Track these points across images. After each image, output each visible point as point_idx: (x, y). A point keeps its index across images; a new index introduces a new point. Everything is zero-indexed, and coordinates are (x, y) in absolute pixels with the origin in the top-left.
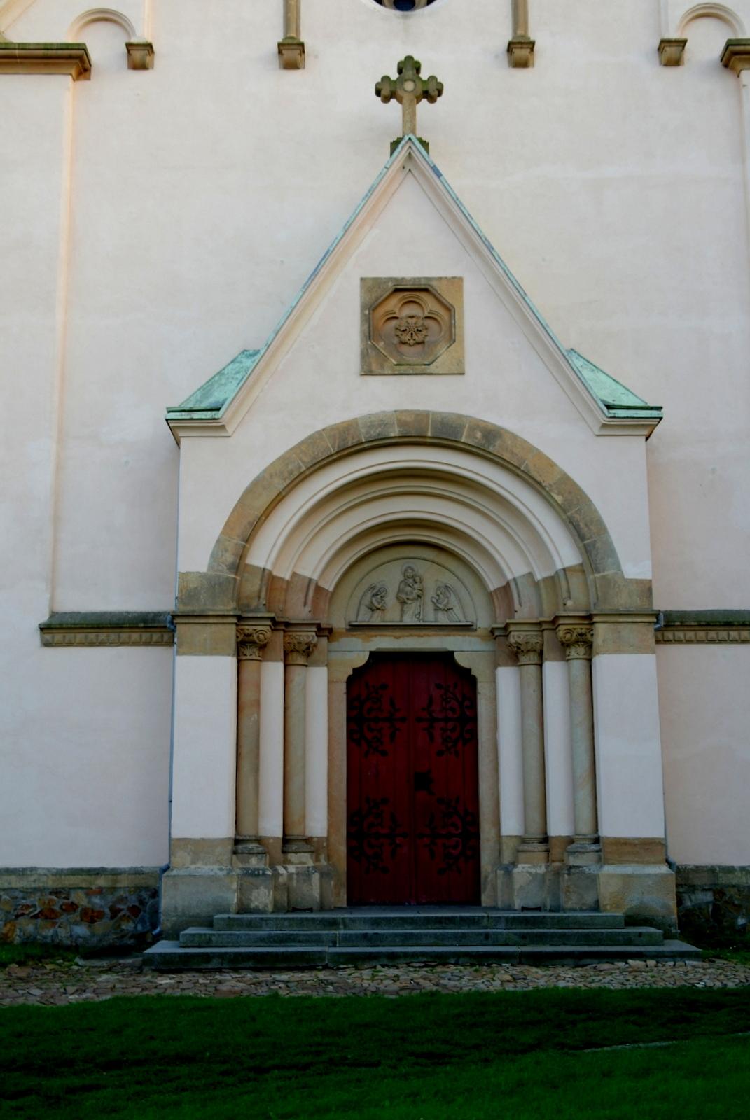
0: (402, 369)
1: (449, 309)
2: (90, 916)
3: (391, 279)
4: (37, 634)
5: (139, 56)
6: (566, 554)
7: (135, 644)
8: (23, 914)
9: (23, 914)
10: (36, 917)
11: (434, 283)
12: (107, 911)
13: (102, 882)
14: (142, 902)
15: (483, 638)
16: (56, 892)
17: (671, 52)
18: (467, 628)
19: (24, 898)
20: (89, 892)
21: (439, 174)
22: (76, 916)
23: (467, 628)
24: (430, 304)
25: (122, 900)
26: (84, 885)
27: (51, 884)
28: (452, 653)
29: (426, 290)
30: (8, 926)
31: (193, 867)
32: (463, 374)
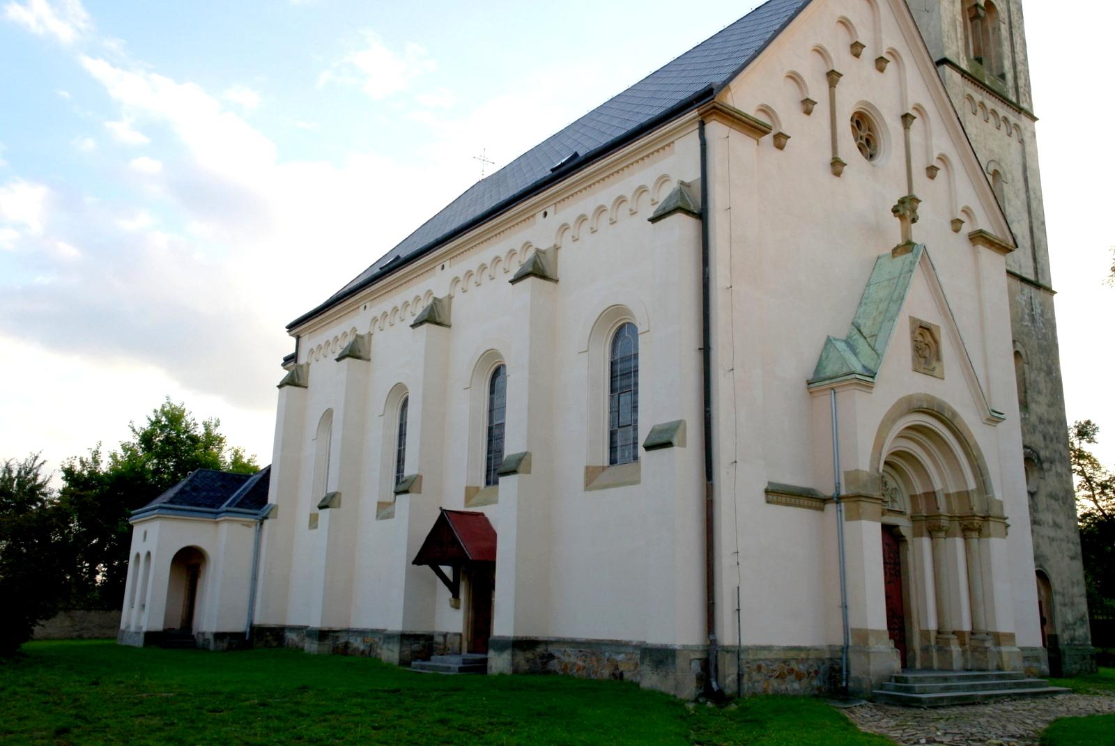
0: (926, 371)
1: (936, 342)
2: (799, 677)
3: (920, 320)
4: (763, 495)
5: (780, 140)
6: (972, 485)
7: (809, 507)
8: (772, 676)
9: (772, 676)
10: (777, 677)
11: (932, 327)
12: (806, 674)
13: (803, 655)
14: (819, 667)
15: (908, 519)
16: (785, 662)
17: (956, 224)
18: (901, 513)
19: (771, 665)
20: (798, 661)
21: (934, 269)
22: (793, 677)
23: (901, 513)
24: (929, 339)
25: (811, 666)
26: (796, 657)
27: (782, 656)
28: (898, 526)
29: (928, 329)
30: (766, 683)
31: (877, 646)
32: (943, 379)
